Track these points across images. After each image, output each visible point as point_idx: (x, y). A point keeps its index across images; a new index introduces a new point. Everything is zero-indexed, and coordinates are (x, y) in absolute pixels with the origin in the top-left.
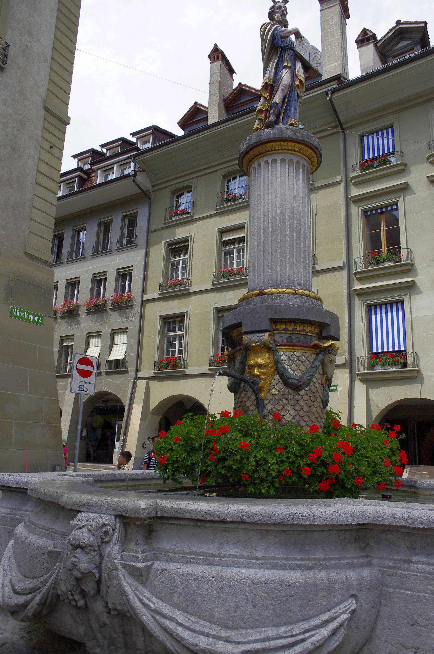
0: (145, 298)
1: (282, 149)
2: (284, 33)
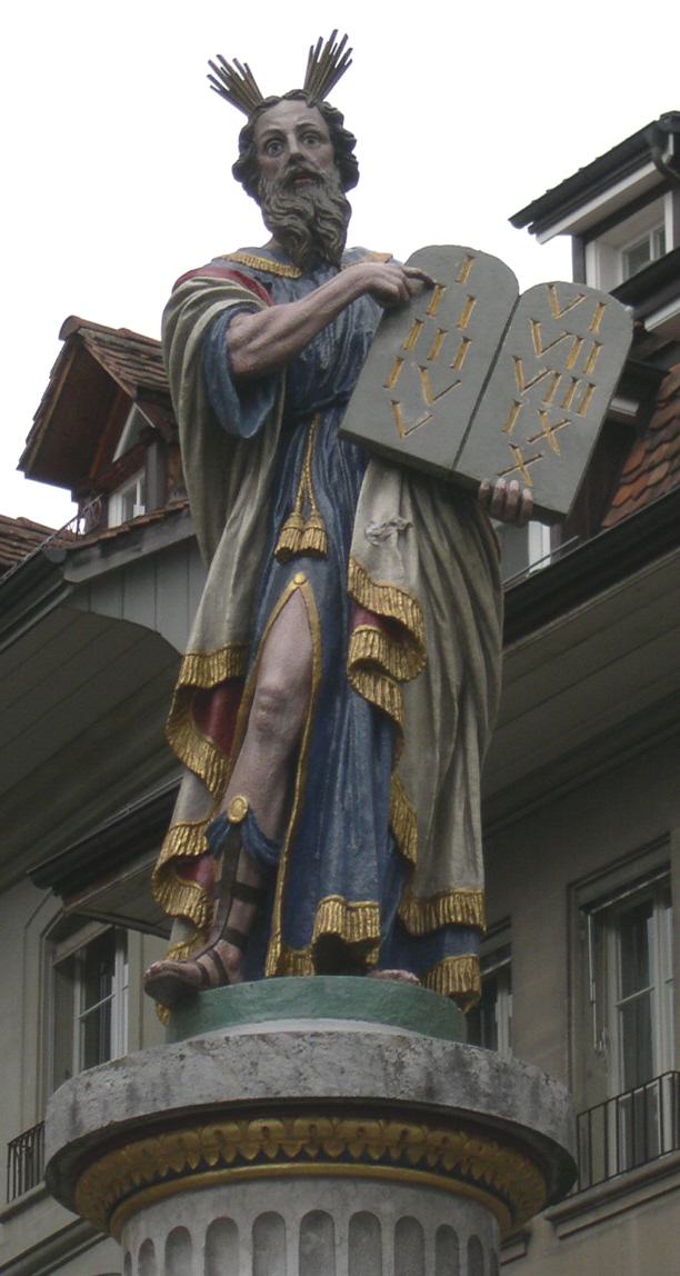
1: (203, 1167)
2: (254, 352)
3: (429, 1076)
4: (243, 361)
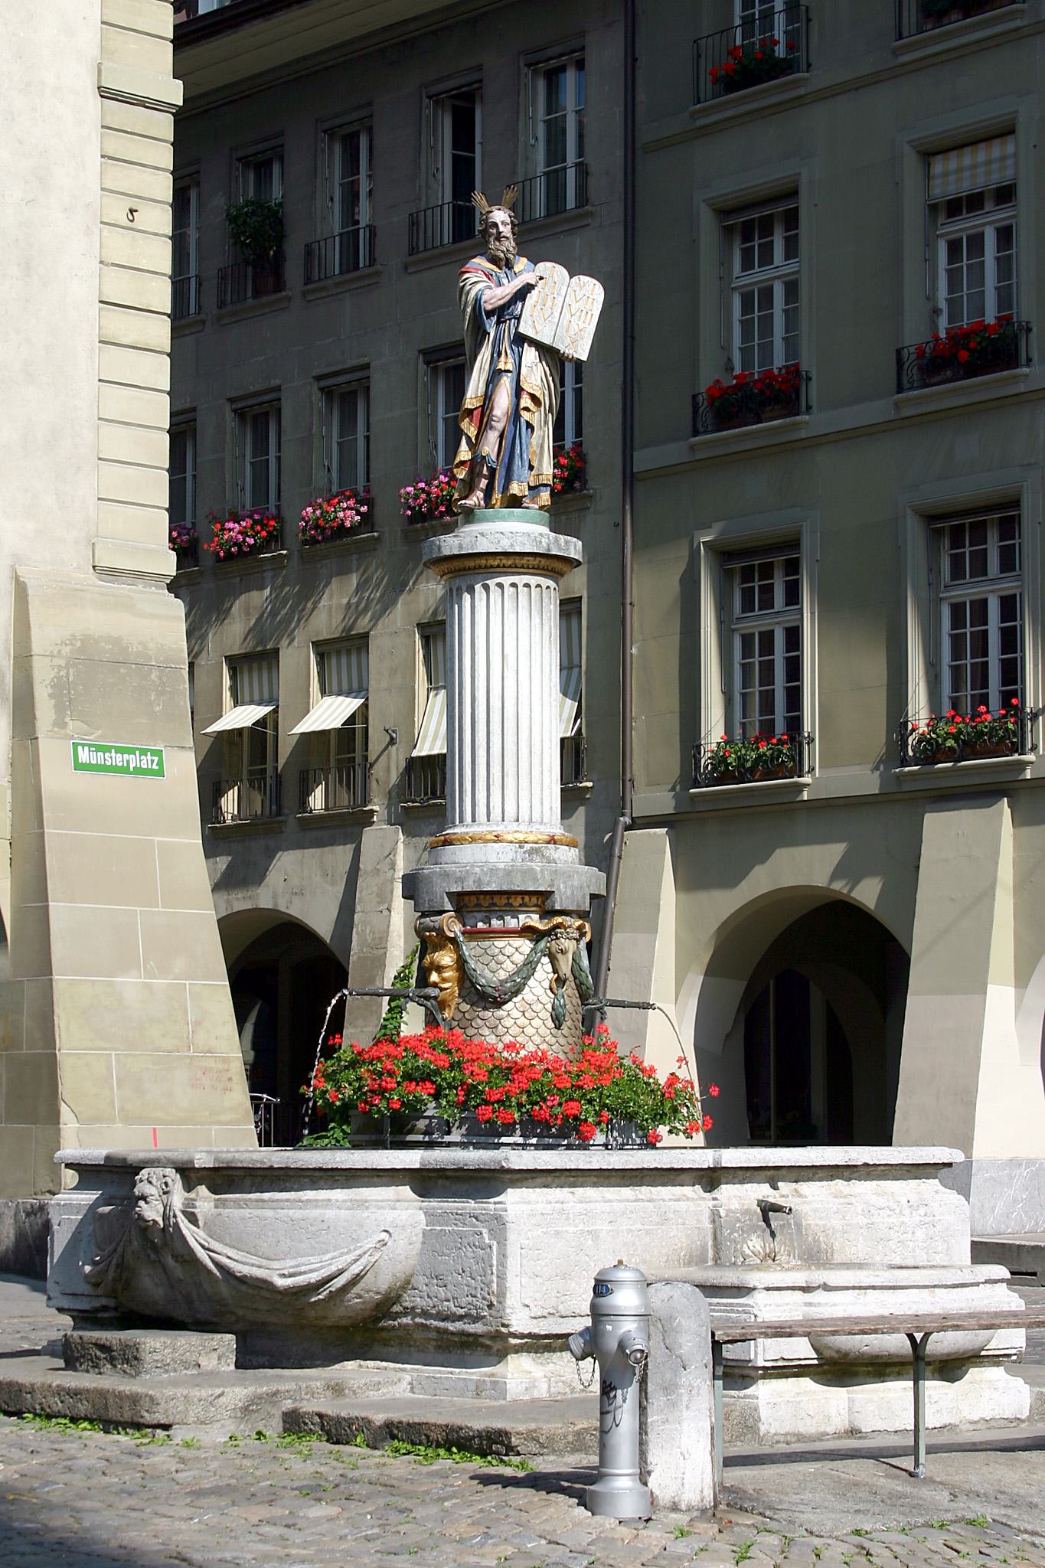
0: (644, 460)
3: (548, 545)
4: (489, 307)
